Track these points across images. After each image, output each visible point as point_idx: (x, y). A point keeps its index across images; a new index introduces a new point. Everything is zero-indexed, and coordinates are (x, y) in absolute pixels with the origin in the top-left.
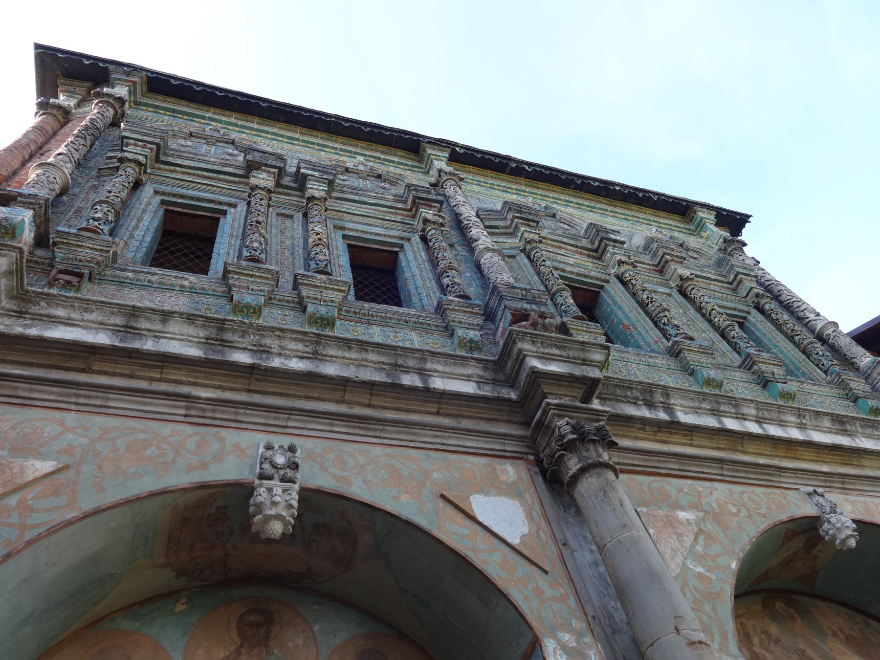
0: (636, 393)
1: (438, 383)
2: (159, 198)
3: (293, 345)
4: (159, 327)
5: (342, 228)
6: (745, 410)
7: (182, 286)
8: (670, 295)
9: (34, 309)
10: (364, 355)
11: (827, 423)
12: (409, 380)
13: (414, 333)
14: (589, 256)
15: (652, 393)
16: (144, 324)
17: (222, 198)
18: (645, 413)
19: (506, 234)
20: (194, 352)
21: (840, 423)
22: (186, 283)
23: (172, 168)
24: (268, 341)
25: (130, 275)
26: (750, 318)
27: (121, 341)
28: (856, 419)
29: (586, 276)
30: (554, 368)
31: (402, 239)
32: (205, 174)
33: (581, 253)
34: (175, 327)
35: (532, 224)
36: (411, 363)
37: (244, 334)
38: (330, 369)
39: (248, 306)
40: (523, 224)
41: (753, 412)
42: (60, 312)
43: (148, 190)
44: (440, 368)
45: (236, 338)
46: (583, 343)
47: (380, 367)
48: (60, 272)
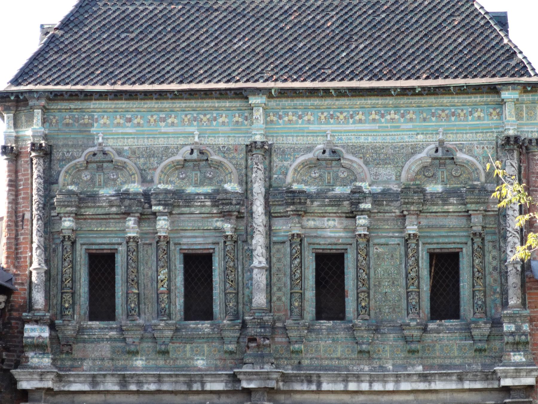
0: (303, 378)
1: (209, 387)
2: (85, 247)
3: (150, 379)
4: (103, 379)
5: (180, 244)
6: (363, 379)
7: (107, 339)
8: (399, 244)
9: (63, 379)
10: (178, 379)
11: (415, 378)
12: (196, 387)
13: (205, 346)
14: (347, 217)
15: (311, 377)
16: (99, 379)
17: (114, 241)
18: (305, 387)
19: (285, 216)
20: (117, 388)
21: (424, 377)
22: (108, 337)
23: (84, 217)
24: (141, 379)
25: (86, 336)
26: (464, 250)
27: (93, 387)
28: (436, 373)
29: (336, 244)
30: (252, 386)
31: (214, 243)
32: (102, 217)
33: (340, 217)
34: (108, 379)
35: (300, 213)
36: (197, 379)
37: (132, 378)
38: (165, 387)
39: (133, 352)
40: (293, 215)
41: (368, 378)
42: (72, 379)
43: (78, 246)
44: (209, 379)
45: (130, 379)
46: (268, 372)
47: (185, 383)
48: (63, 345)
